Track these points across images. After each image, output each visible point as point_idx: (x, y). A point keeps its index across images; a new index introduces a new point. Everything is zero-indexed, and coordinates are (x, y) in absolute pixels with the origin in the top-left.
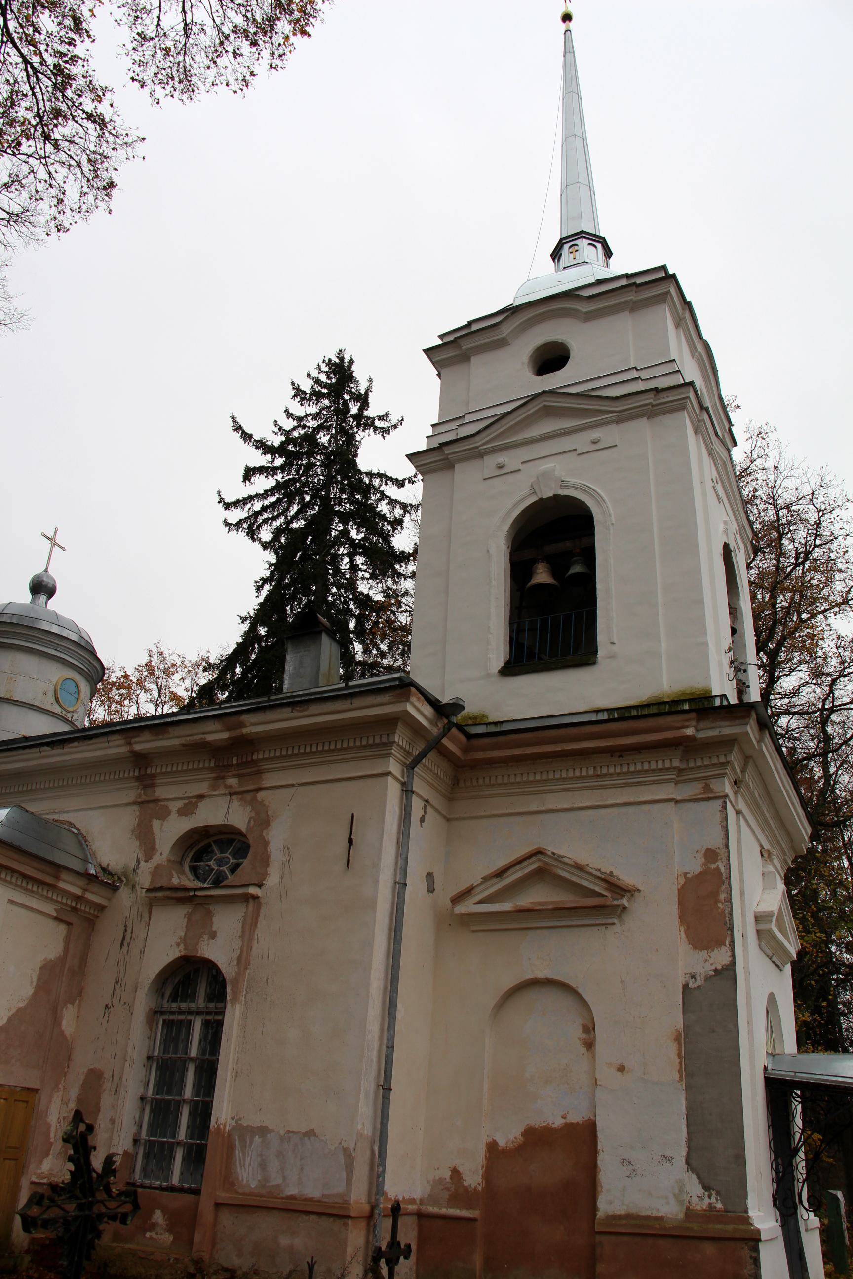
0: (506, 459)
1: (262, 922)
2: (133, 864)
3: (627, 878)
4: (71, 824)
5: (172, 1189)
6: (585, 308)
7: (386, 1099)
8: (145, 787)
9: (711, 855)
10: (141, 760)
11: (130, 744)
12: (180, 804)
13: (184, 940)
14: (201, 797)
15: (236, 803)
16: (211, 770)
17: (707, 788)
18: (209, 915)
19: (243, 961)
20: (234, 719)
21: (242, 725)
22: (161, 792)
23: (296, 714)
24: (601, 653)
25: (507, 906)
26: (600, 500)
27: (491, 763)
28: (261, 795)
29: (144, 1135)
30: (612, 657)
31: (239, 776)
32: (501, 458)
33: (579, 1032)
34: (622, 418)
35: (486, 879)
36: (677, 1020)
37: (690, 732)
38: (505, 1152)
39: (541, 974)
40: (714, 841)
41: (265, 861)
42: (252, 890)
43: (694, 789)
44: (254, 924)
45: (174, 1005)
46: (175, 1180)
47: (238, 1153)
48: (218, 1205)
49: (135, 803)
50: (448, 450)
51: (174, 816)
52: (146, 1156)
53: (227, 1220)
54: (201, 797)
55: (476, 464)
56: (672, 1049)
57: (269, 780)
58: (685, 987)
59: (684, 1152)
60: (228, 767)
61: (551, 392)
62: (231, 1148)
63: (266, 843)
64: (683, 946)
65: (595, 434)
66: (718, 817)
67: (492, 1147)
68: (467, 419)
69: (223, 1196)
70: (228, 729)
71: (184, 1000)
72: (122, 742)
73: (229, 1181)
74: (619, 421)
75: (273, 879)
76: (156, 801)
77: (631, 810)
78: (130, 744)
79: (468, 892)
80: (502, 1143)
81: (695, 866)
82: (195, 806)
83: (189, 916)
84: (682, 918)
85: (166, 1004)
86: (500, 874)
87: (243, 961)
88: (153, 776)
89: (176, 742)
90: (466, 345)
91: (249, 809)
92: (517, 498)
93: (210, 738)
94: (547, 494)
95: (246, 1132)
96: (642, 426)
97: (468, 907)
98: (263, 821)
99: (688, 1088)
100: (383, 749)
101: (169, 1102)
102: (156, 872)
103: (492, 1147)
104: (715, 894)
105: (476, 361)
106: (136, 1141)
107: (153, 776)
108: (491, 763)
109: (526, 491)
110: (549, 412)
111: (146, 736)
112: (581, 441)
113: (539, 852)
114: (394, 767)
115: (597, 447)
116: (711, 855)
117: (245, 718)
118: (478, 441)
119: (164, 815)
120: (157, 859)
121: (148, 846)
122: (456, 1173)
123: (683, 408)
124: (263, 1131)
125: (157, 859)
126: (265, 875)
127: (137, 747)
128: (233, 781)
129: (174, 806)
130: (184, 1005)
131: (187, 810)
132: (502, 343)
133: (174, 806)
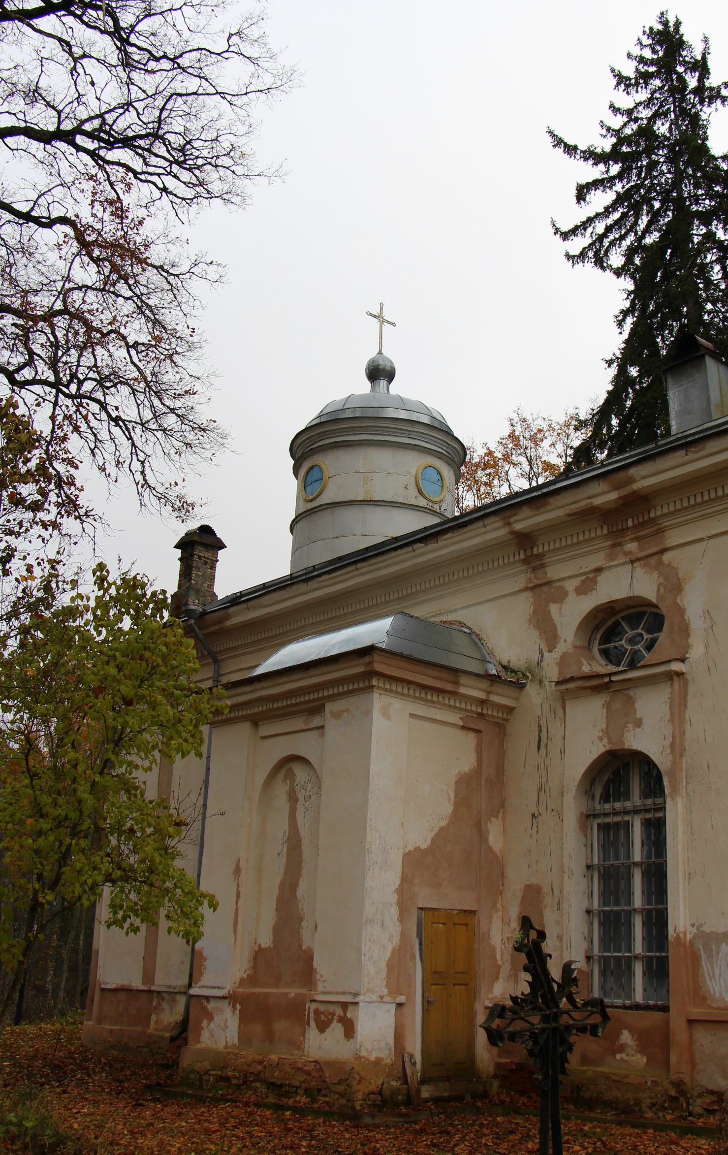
1: (691, 701)
2: (536, 657)
4: (461, 624)
5: (637, 1007)
8: (534, 569)
10: (524, 540)
11: (509, 524)
12: (576, 582)
13: (607, 733)
14: (599, 570)
16: (606, 537)
18: (630, 701)
19: (677, 748)
20: (621, 475)
21: (632, 480)
22: (554, 572)
23: (691, 457)
28: (667, 557)
29: (596, 951)
31: (637, 539)
41: (685, 631)
42: (675, 666)
44: (683, 704)
45: (607, 807)
46: (639, 997)
47: (704, 962)
48: (691, 1022)
49: (526, 589)
51: (572, 596)
52: (603, 973)
53: (703, 1038)
54: (599, 570)
57: (674, 538)
60: (623, 531)
62: (695, 959)
63: (682, 611)
69: (695, 1012)
70: (617, 488)
71: (617, 799)
72: (499, 524)
73: (699, 995)
75: (696, 651)
76: (549, 583)
78: (509, 524)
82: (594, 581)
83: (608, 706)
85: (598, 807)
87: (677, 748)
88: (541, 556)
89: (560, 513)
91: (655, 575)
93: (597, 501)
101: (618, 914)
102: (563, 661)
106: (588, 958)
107: (541, 556)
111: (526, 512)
117: (632, 471)
119: (560, 597)
121: (551, 637)
126: (687, 647)
127: (518, 527)
128: (632, 546)
129: (570, 586)
130: (618, 805)
131: (587, 586)
133: (570, 586)
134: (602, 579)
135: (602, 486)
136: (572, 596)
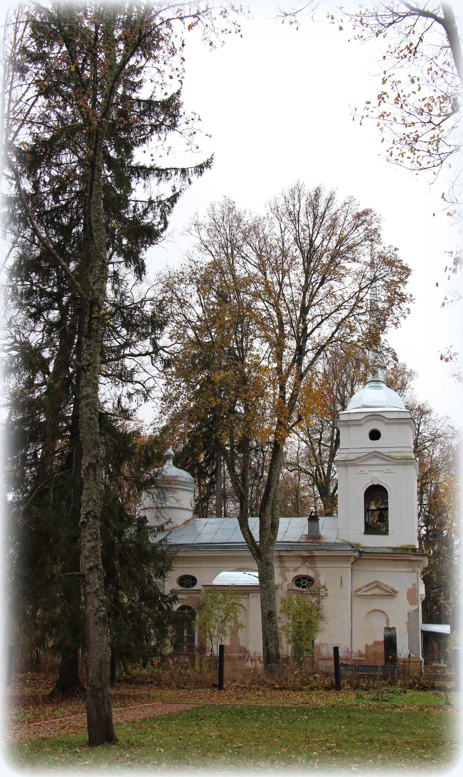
0: (365, 469)
2: (281, 583)
3: (396, 589)
6: (386, 421)
7: (351, 637)
9: (414, 585)
12: (293, 569)
14: (299, 567)
15: (309, 570)
17: (414, 570)
22: (287, 564)
24: (389, 532)
25: (369, 593)
26: (390, 489)
27: (364, 559)
28: (316, 569)
30: (392, 534)
32: (362, 468)
33: (385, 621)
34: (396, 464)
35: (364, 587)
36: (406, 620)
37: (412, 558)
38: (369, 646)
39: (377, 609)
40: (415, 582)
43: (411, 569)
47: (321, 648)
48: (318, 659)
50: (346, 462)
51: (291, 571)
53: (320, 662)
54: (299, 567)
55: (354, 468)
56: (406, 626)
57: (318, 565)
58: (408, 613)
59: (407, 646)
60: (306, 561)
61: (379, 452)
62: (319, 648)
63: (319, 581)
64: (408, 604)
65: (389, 467)
66: (416, 576)
67: (367, 645)
68: (351, 451)
69: (320, 657)
73: (320, 654)
74: (395, 465)
77: (397, 573)
79: (359, 590)
80: (369, 644)
81: (411, 587)
84: (408, 598)
86: (368, 586)
90: (349, 423)
92: (367, 482)
94: (375, 484)
95: (323, 645)
96: (401, 467)
97: (360, 593)
98: (318, 575)
99: (409, 634)
100: (348, 561)
102: (288, 585)
103: (367, 645)
104: (415, 594)
105: (352, 428)
108: (364, 559)
109: (370, 481)
110: (376, 456)
111: (285, 552)
112: (385, 468)
113: (377, 582)
114: (349, 565)
115: (389, 471)
116: (414, 585)
118: (355, 462)
119: (288, 571)
120: (288, 582)
121: (285, 579)
122: (359, 651)
123: (412, 464)
124: (327, 644)
125: (288, 582)
128: (308, 564)
129: (291, 569)
131: (296, 570)
132: (360, 425)
133: (291, 569)
134: (299, 569)
135: (306, 552)
136: (291, 571)
